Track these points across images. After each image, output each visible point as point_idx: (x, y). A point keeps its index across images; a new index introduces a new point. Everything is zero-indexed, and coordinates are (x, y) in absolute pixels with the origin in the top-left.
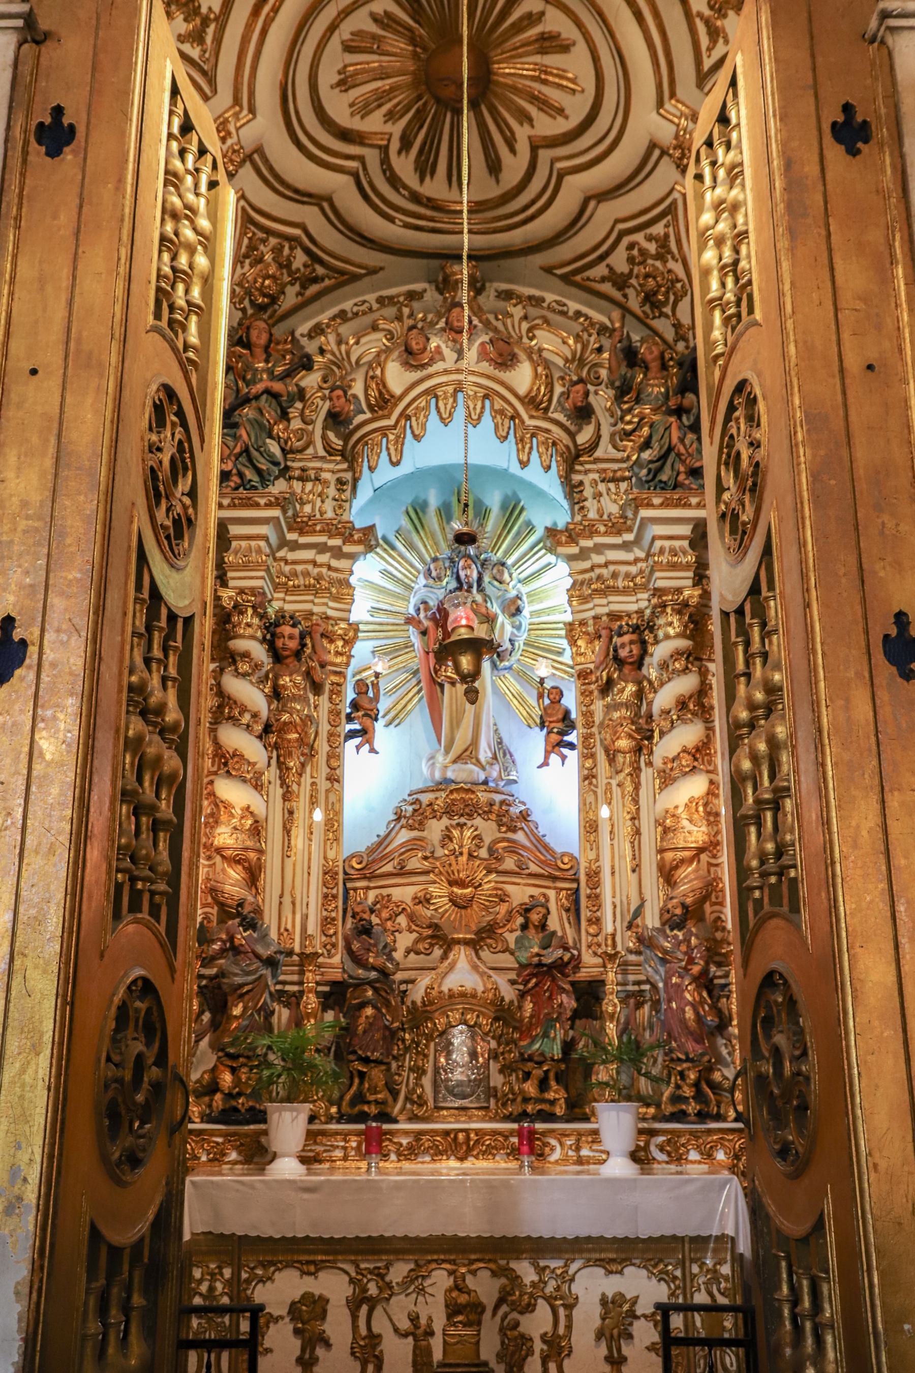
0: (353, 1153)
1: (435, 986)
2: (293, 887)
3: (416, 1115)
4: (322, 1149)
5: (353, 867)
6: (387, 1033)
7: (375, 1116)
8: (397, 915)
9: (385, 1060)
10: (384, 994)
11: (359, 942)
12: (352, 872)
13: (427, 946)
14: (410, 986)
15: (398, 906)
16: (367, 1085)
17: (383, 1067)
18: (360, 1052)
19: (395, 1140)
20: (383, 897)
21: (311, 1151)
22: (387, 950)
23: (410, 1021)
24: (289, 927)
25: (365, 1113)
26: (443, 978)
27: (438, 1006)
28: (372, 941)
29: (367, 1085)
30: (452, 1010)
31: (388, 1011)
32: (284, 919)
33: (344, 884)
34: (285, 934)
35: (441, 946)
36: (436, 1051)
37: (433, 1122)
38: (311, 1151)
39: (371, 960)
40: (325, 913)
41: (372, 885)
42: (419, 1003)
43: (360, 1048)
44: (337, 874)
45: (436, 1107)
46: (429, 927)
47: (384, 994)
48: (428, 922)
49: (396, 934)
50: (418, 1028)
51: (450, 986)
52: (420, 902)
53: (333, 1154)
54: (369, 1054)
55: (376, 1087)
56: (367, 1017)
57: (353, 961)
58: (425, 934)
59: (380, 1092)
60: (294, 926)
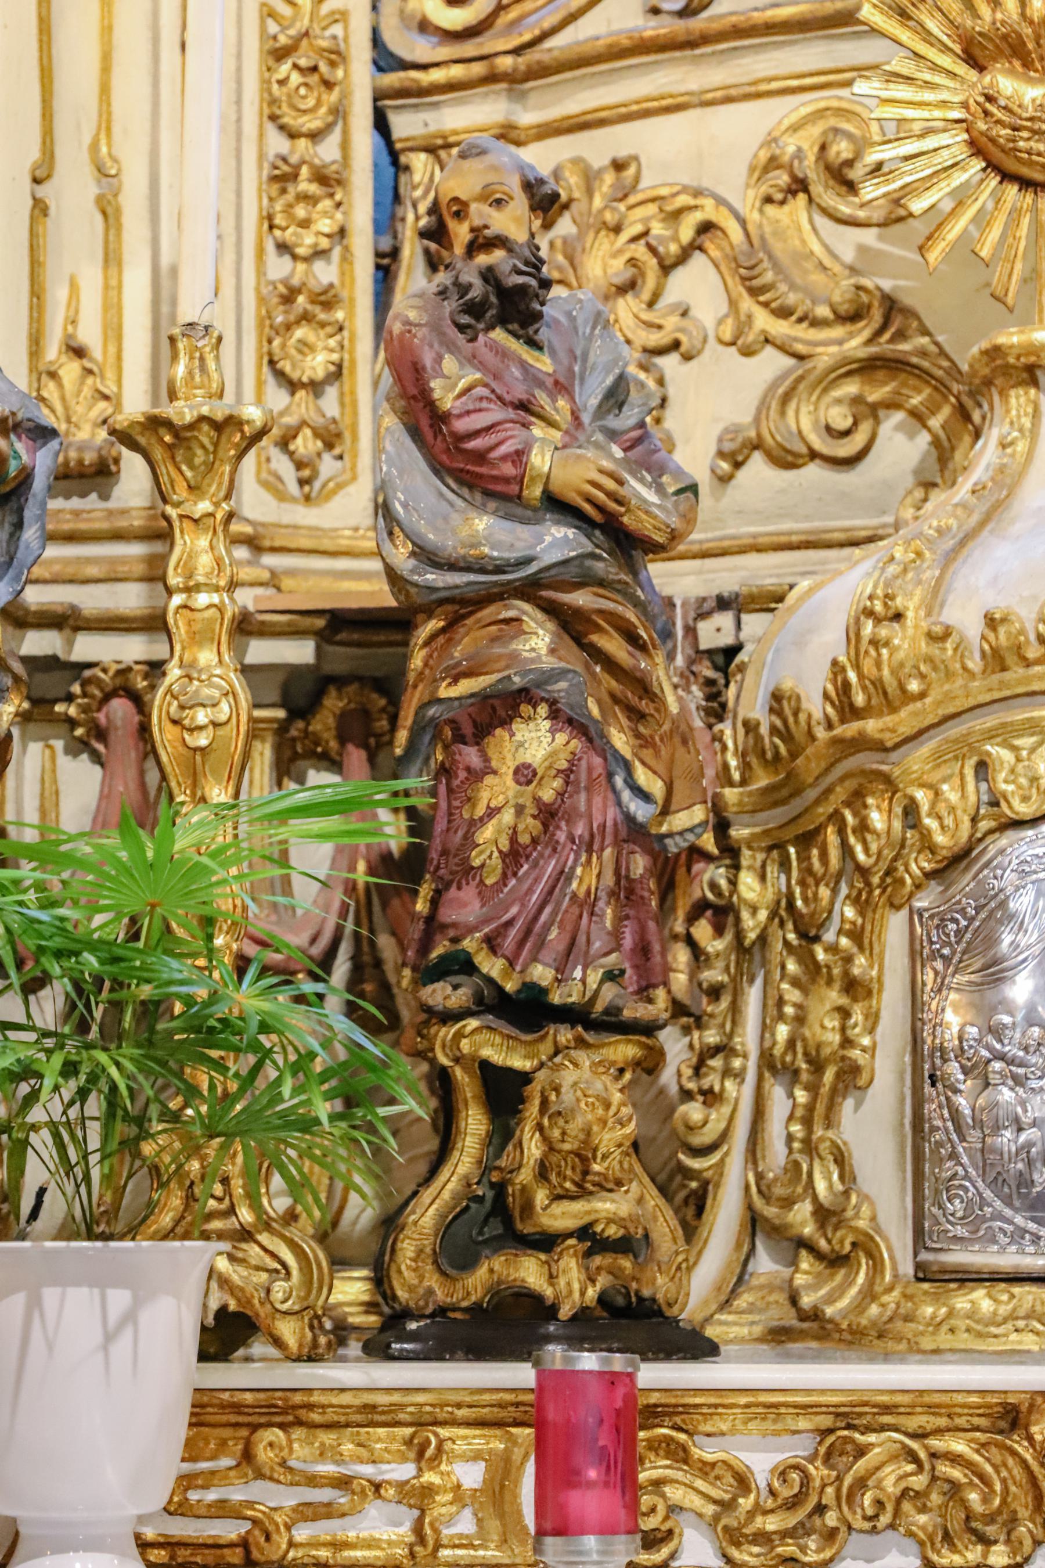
0: (465, 1524)
1: (910, 604)
2: (105, 122)
3: (815, 1315)
4: (288, 1498)
5: (424, 26)
6: (639, 864)
7: (582, 1316)
8: (666, 268)
9: (634, 1011)
10: (614, 645)
11: (473, 360)
12: (421, 49)
13: (840, 418)
14: (754, 624)
15: (677, 215)
16: (533, 1149)
17: (625, 1050)
18: (492, 966)
19: (706, 1451)
20: (590, 179)
21: (222, 1510)
22: (627, 419)
23: (771, 798)
24: (89, 334)
25: (534, 1298)
26: (950, 558)
27: (927, 710)
28: (544, 364)
29: (533, 1149)
30: (1004, 734)
31: (644, 742)
32: (58, 295)
33: (381, 124)
34: (70, 370)
35: (918, 417)
36: (916, 955)
37: (916, 1351)
38: (222, 1510)
39: (540, 460)
40: (279, 267)
41: (528, 117)
42: (815, 706)
43: (492, 944)
44: (337, 56)
45: (923, 1274)
46: (853, 316)
47: (614, 645)
48: (841, 292)
49: (669, 363)
50: (807, 840)
51: (997, 602)
52: (799, 186)
53: (351, 1530)
54: (542, 974)
55: (584, 1157)
56: (525, 775)
57: (438, 469)
58: (826, 356)
59: (610, 1185)
60: (113, 330)
